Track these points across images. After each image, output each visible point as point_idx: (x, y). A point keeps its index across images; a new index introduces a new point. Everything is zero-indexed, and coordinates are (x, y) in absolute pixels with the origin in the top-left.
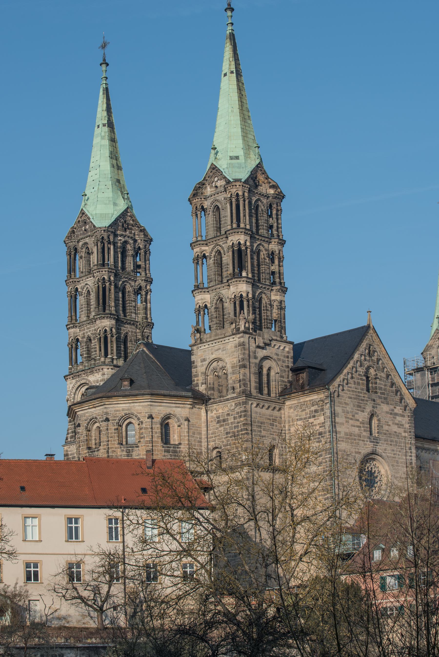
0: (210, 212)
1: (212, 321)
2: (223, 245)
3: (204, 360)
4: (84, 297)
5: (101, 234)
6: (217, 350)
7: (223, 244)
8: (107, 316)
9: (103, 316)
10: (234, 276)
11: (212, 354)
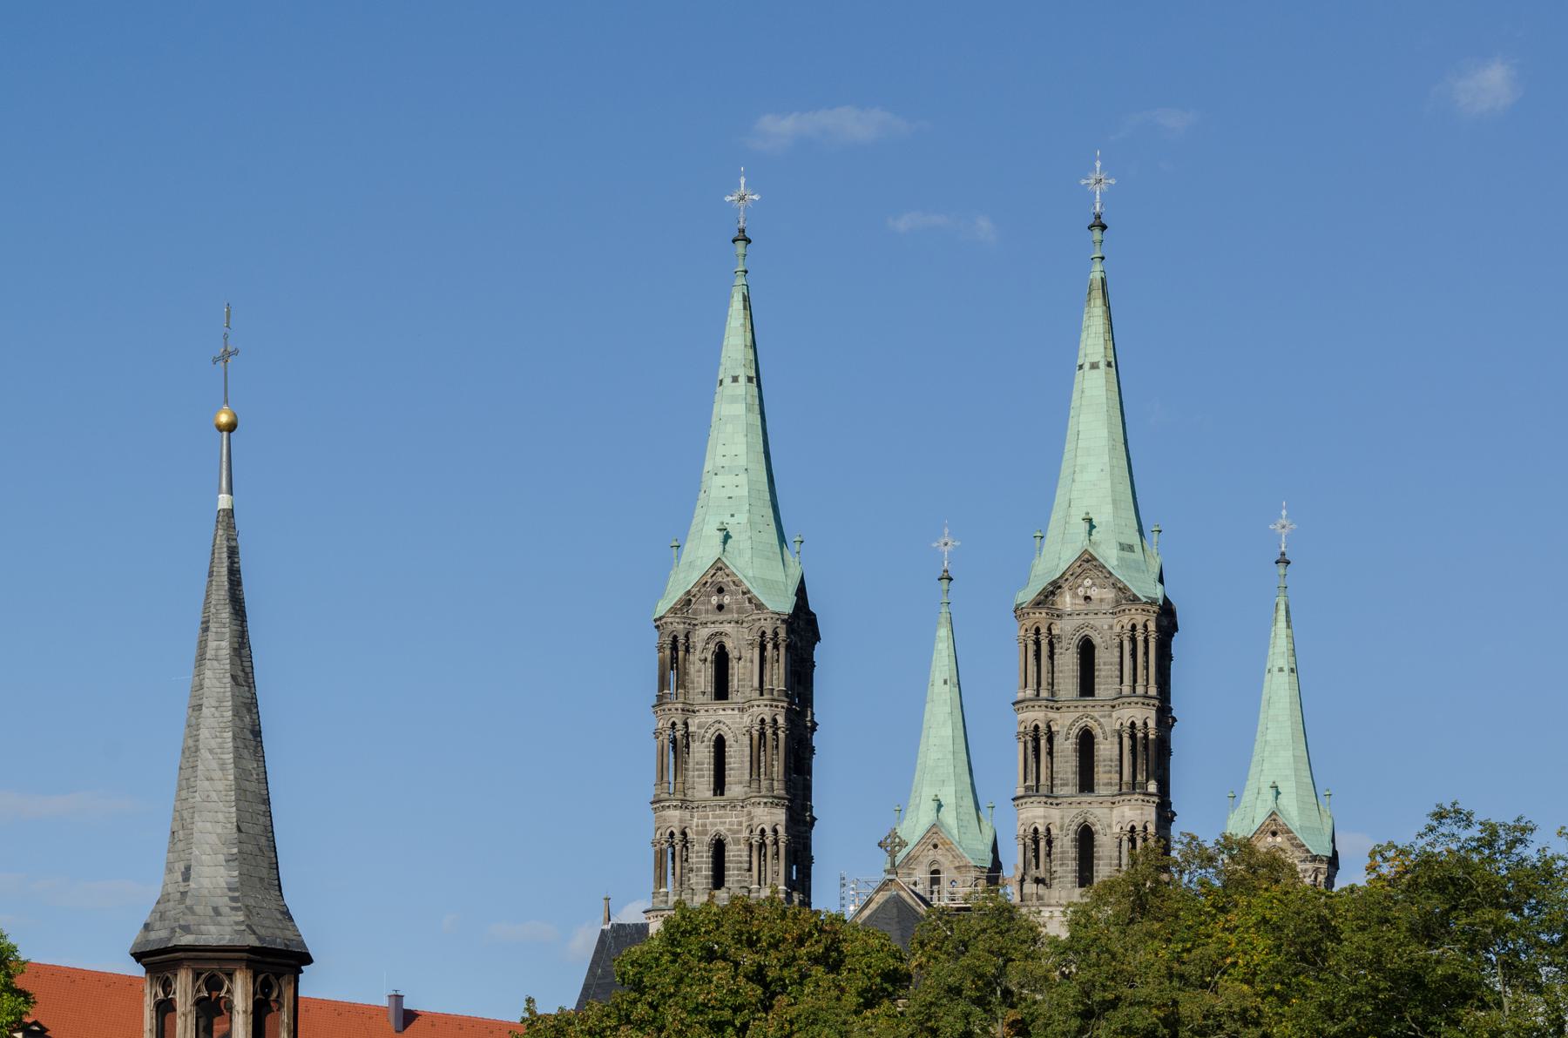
0: (1071, 646)
1: (1063, 864)
2: (1102, 720)
4: (709, 747)
5: (775, 626)
7: (1101, 717)
8: (783, 802)
9: (776, 801)
10: (1134, 789)
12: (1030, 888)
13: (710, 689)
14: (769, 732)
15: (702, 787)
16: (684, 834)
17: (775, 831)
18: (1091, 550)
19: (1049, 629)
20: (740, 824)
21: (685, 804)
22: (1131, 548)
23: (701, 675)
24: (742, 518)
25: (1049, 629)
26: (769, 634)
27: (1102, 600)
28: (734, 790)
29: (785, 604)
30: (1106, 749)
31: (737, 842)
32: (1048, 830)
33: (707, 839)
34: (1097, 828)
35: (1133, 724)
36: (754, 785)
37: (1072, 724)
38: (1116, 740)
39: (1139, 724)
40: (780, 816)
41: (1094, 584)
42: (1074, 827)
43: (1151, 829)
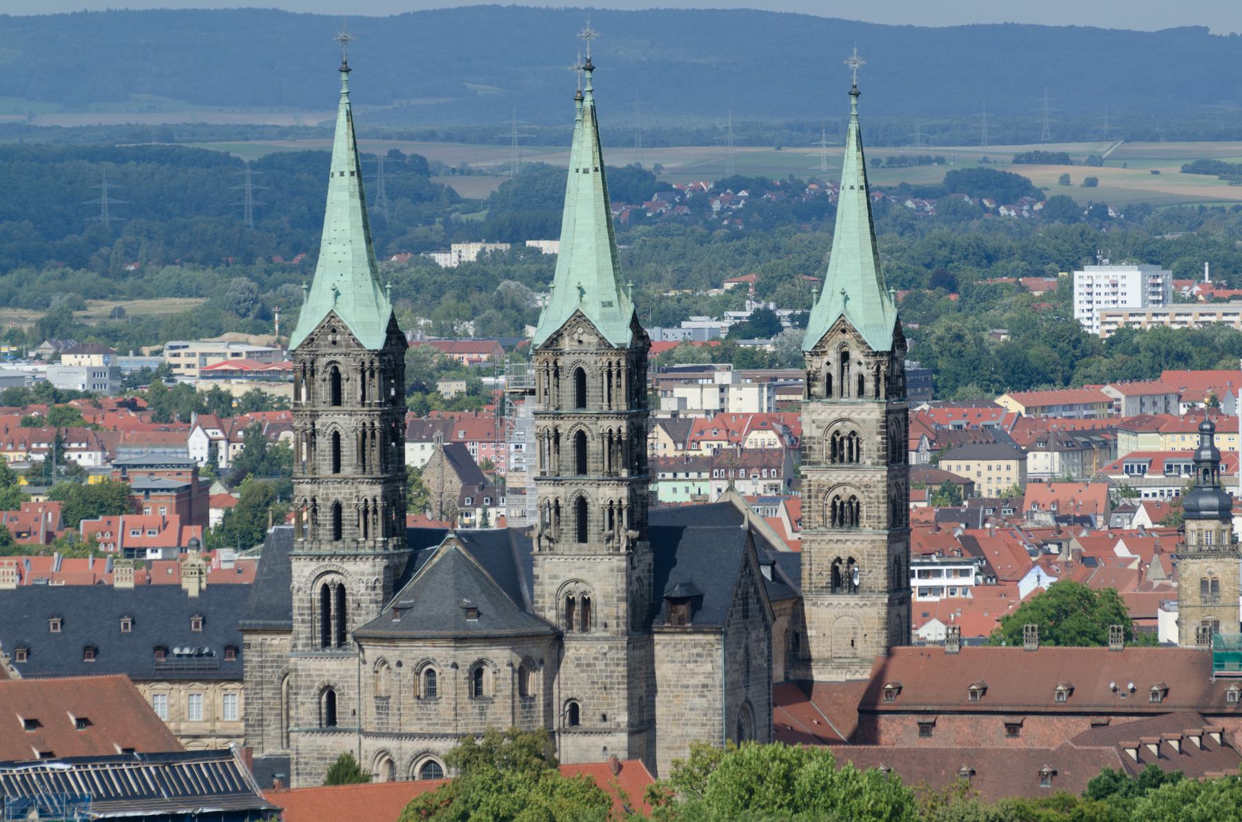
3: (555, 577)
6: (579, 568)
11: (570, 571)
12: (544, 542)
13: (329, 399)
14: (369, 433)
15: (326, 469)
16: (314, 500)
17: (375, 500)
18: (581, 310)
19: (555, 363)
20: (351, 494)
21: (314, 481)
22: (610, 304)
23: (324, 391)
24: (348, 277)
25: (555, 363)
26: (367, 365)
27: (589, 343)
28: (347, 470)
29: (375, 340)
30: (594, 446)
31: (349, 506)
32: (557, 501)
33: (330, 504)
34: (589, 500)
35: (610, 431)
36: (360, 470)
37: (571, 429)
38: (600, 440)
39: (615, 431)
40: (378, 490)
41: (584, 332)
42: (574, 499)
43: (624, 502)
